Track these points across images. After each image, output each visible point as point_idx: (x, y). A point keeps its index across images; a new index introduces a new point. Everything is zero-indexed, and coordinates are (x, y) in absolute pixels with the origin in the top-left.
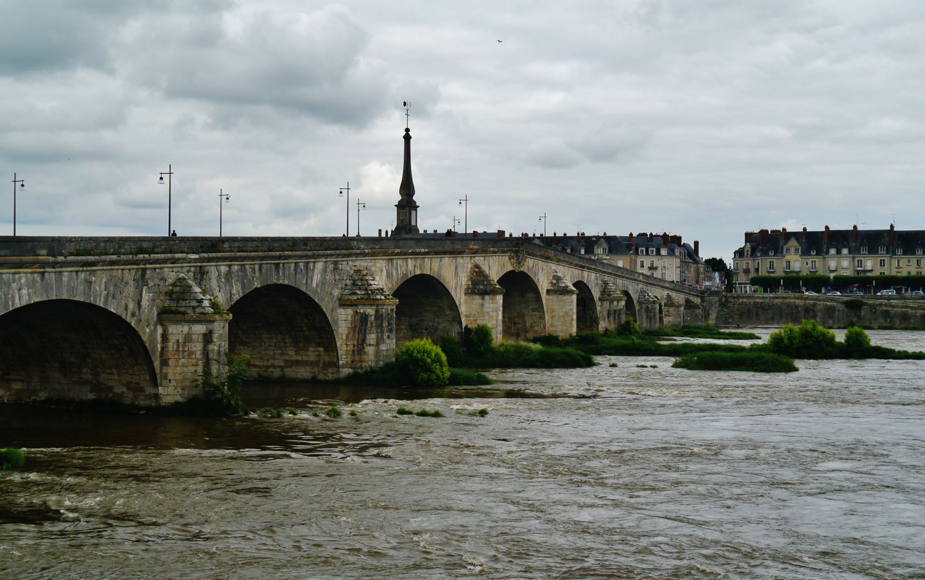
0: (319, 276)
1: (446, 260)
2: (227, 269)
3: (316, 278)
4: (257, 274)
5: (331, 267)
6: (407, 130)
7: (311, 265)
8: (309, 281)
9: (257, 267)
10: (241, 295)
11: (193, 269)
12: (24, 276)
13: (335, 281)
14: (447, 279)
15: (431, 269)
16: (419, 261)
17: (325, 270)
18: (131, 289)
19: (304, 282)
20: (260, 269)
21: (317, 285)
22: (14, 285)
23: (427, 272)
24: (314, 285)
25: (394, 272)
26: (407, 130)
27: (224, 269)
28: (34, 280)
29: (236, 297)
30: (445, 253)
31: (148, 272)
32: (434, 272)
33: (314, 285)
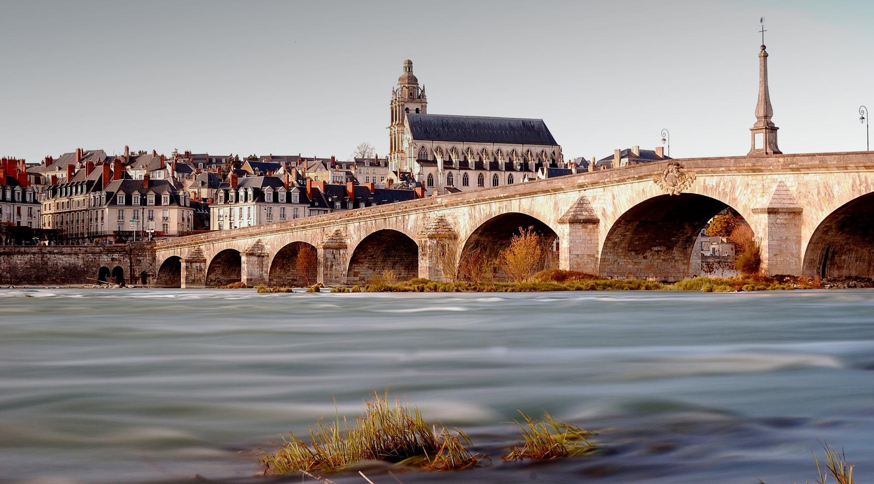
0: (412, 223)
1: (541, 199)
2: (358, 224)
3: (410, 224)
4: (374, 225)
5: (421, 216)
6: (764, 47)
7: (407, 217)
8: (405, 227)
9: (373, 221)
10: (366, 236)
11: (343, 226)
12: (288, 234)
13: (424, 225)
14: (542, 214)
15: (520, 208)
16: (505, 203)
17: (417, 220)
18: (319, 236)
19: (402, 227)
20: (376, 223)
21: (411, 228)
22: (286, 237)
23: (515, 210)
24: (409, 228)
25: (477, 215)
26: (764, 47)
27: (357, 224)
28: (291, 235)
29: (363, 238)
30: (536, 193)
31: (325, 228)
32: (524, 210)
33: (409, 228)
